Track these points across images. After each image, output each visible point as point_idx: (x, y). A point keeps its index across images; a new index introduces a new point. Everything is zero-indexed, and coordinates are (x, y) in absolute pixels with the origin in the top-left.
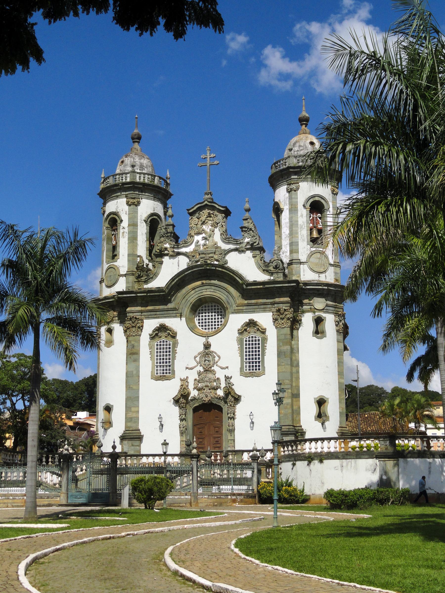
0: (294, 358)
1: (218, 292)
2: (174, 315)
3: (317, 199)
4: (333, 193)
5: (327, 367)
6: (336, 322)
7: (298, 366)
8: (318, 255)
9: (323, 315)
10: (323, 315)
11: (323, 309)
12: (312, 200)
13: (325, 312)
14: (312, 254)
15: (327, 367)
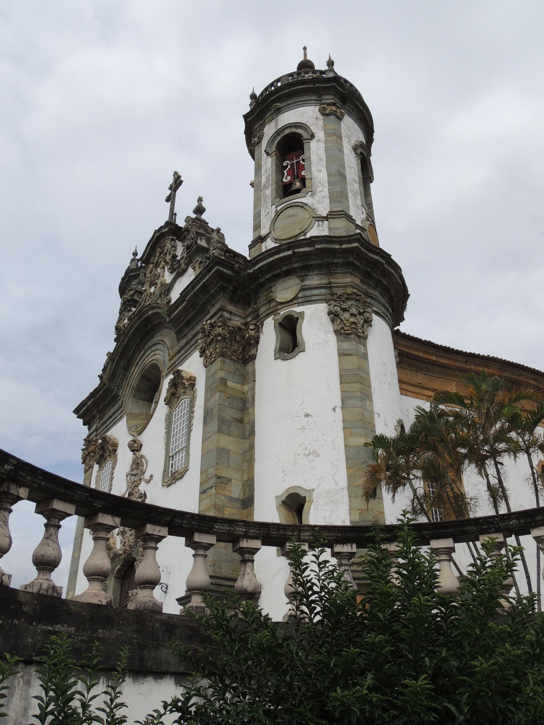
0: (246, 420)
1: (158, 352)
2: (119, 417)
3: (287, 132)
4: (323, 115)
5: (307, 415)
6: (330, 313)
7: (252, 432)
8: (290, 211)
9: (298, 309)
10: (298, 309)
11: (296, 298)
12: (279, 138)
13: (300, 304)
14: (278, 214)
15: (307, 415)
